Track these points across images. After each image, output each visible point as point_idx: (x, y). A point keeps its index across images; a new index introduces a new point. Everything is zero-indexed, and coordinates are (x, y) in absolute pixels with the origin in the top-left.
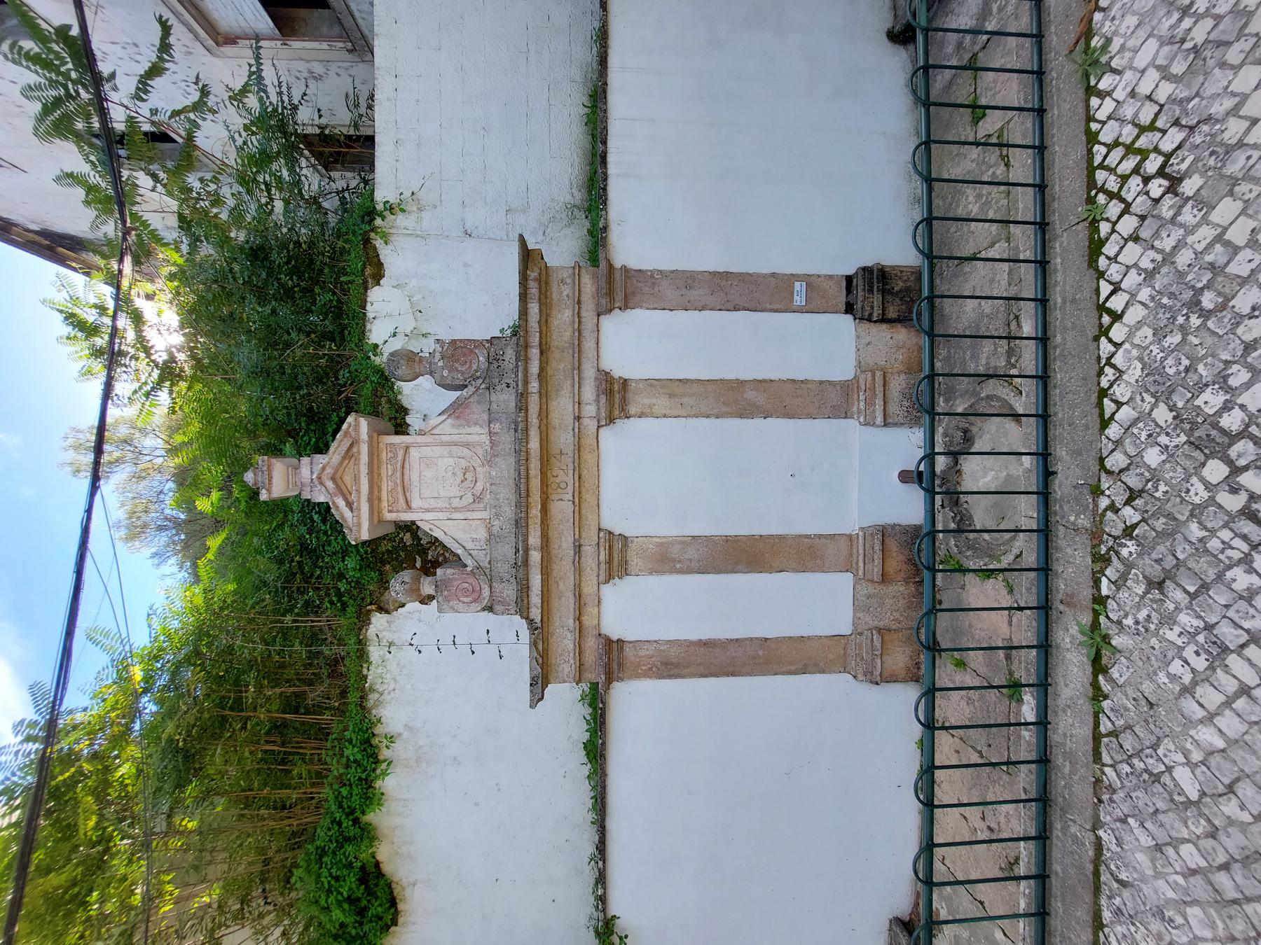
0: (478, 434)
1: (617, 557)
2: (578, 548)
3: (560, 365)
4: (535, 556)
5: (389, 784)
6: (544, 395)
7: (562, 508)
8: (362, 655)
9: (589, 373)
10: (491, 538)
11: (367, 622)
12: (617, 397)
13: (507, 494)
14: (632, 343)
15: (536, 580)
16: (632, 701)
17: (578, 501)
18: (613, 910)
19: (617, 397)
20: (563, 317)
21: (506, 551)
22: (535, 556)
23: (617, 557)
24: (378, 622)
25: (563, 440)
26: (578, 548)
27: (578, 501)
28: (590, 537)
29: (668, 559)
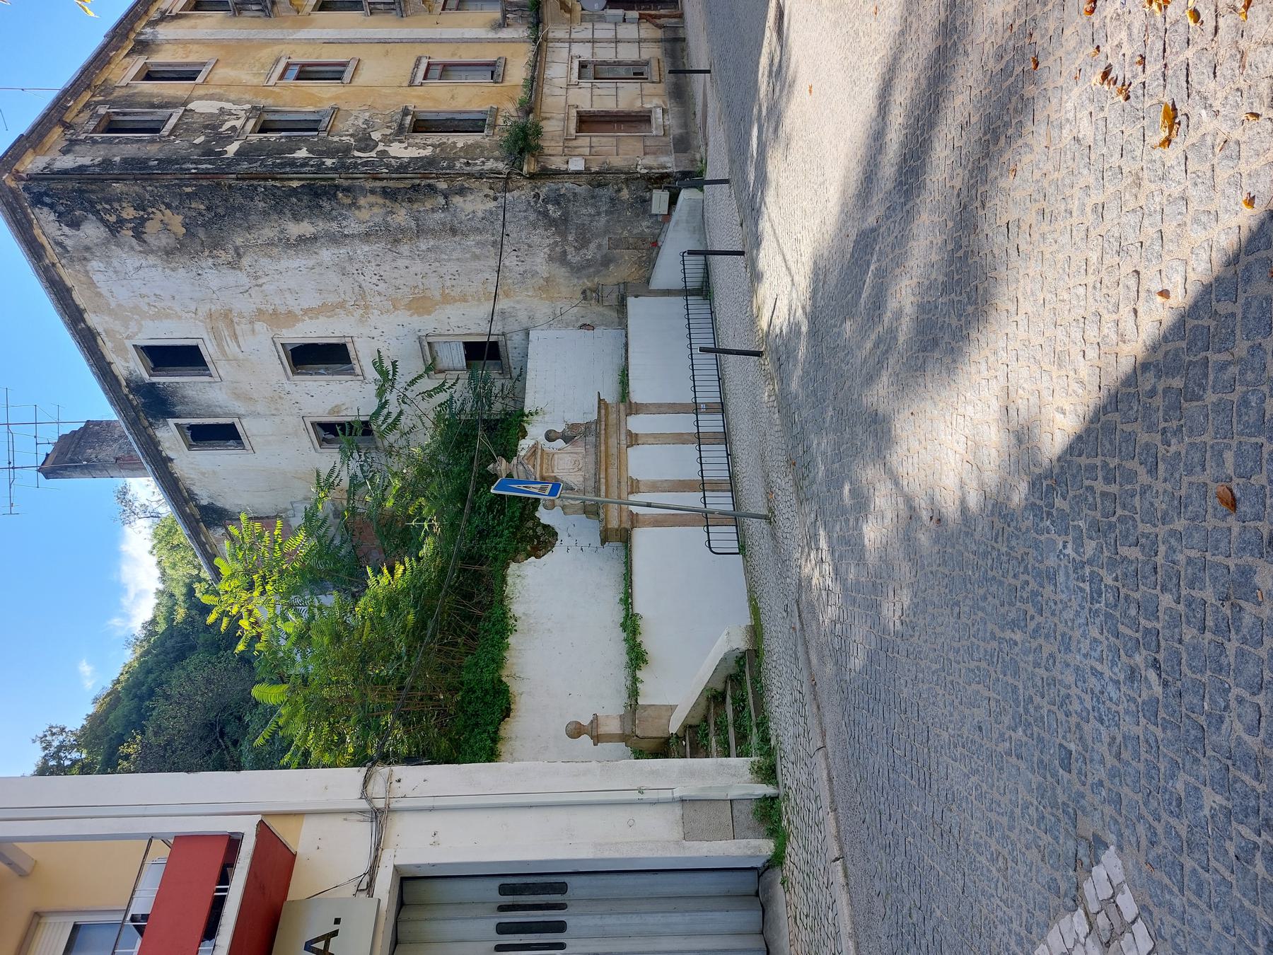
0: (581, 450)
1: (635, 486)
2: (619, 482)
3: (612, 430)
4: (603, 481)
5: (511, 640)
6: (606, 438)
7: (613, 471)
8: (504, 581)
11: (508, 566)
12: (634, 439)
13: (592, 467)
14: (636, 423)
16: (643, 539)
17: (619, 468)
18: (639, 607)
19: (634, 439)
20: (613, 417)
22: (603, 481)
24: (513, 566)
25: (614, 451)
26: (619, 482)
27: (619, 468)
28: (624, 480)
29: (655, 487)
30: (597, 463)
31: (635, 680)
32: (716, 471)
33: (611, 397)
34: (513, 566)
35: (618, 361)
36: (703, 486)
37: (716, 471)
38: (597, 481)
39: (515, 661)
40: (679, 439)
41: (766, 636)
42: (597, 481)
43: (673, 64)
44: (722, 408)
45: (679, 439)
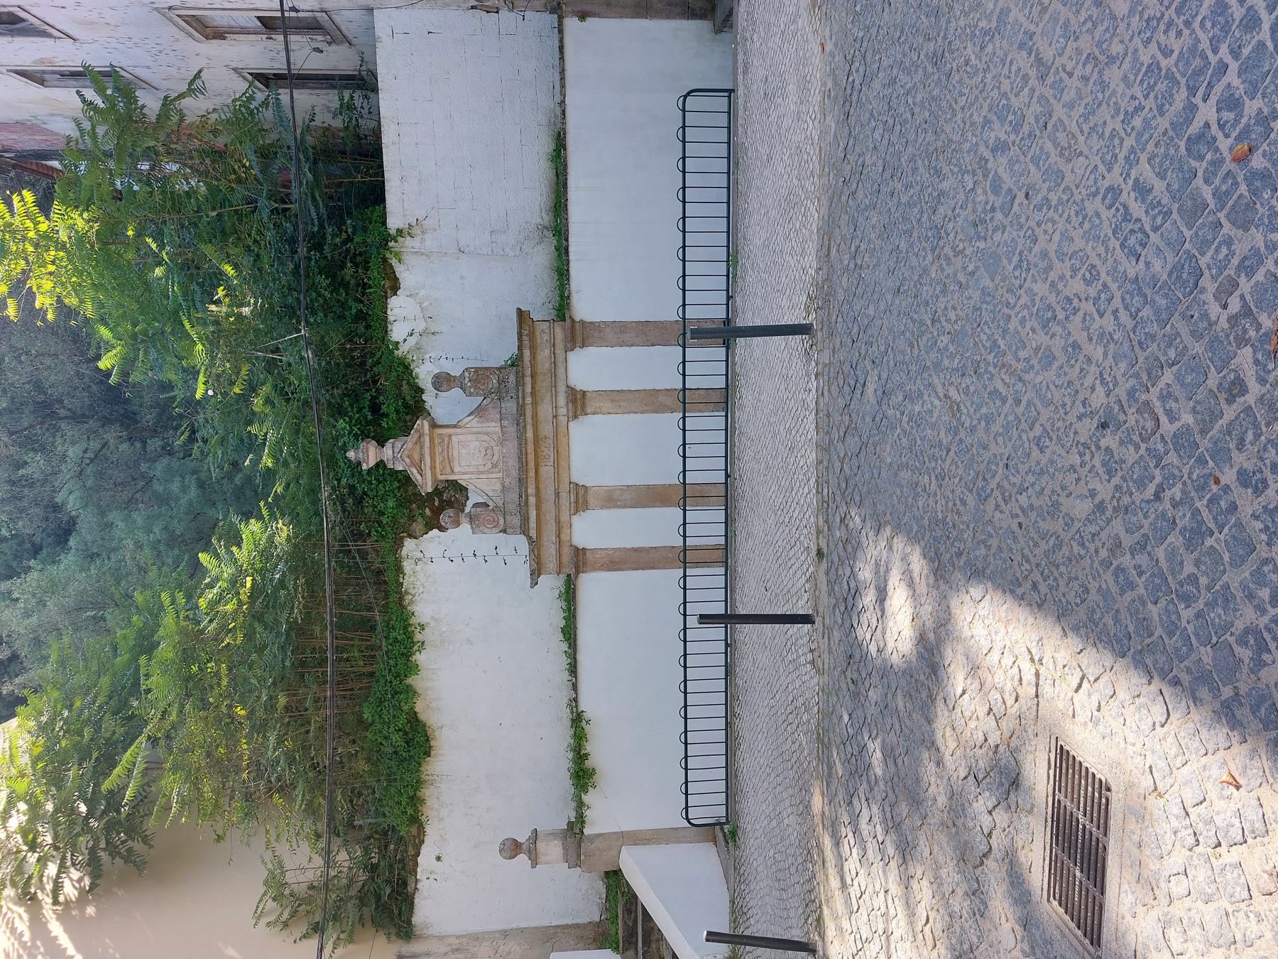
0: (494, 427)
1: (581, 499)
2: (557, 494)
3: (543, 384)
4: (532, 500)
5: (420, 658)
6: (534, 403)
7: (547, 471)
8: (399, 569)
9: (562, 388)
10: (504, 489)
11: (399, 544)
12: (579, 402)
13: (513, 463)
14: (587, 368)
15: (533, 514)
16: (592, 585)
17: (557, 466)
18: (583, 706)
19: (579, 402)
20: (544, 354)
21: (514, 496)
22: (532, 500)
23: (581, 499)
24: (409, 545)
25: (547, 429)
26: (557, 494)
27: (557, 466)
28: (564, 487)
29: (612, 499)
30: (523, 467)
31: (580, 805)
32: (706, 471)
33: (540, 311)
34: (409, 544)
35: (547, 102)
36: (684, 495)
37: (706, 471)
38: (523, 495)
39: (428, 684)
40: (649, 401)
41: (742, 504)
42: (523, 495)
43: (737, 911)
44: (727, 496)
45: (649, 401)
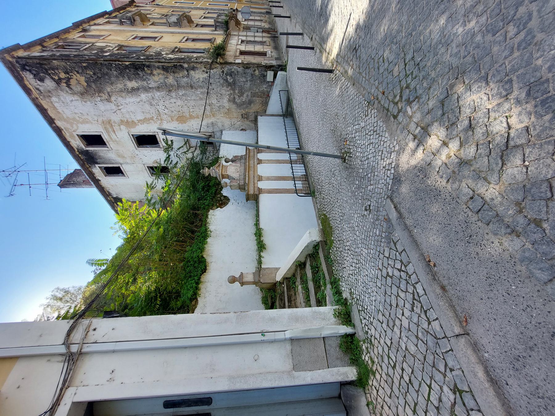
1: (260, 179)
2: (254, 177)
3: (251, 158)
4: (247, 176)
5: (209, 240)
6: (249, 161)
7: (251, 173)
8: (207, 217)
9: (256, 159)
10: (240, 175)
12: (260, 162)
13: (243, 171)
14: (261, 156)
15: (247, 178)
16: (263, 198)
17: (254, 172)
18: (262, 226)
19: (260, 162)
20: (252, 154)
21: (243, 177)
22: (247, 176)
23: (260, 179)
24: (211, 211)
25: (252, 165)
26: (254, 177)
27: (254, 172)
28: (256, 175)
29: (268, 179)
30: (245, 169)
31: (260, 257)
39: (209, 248)
